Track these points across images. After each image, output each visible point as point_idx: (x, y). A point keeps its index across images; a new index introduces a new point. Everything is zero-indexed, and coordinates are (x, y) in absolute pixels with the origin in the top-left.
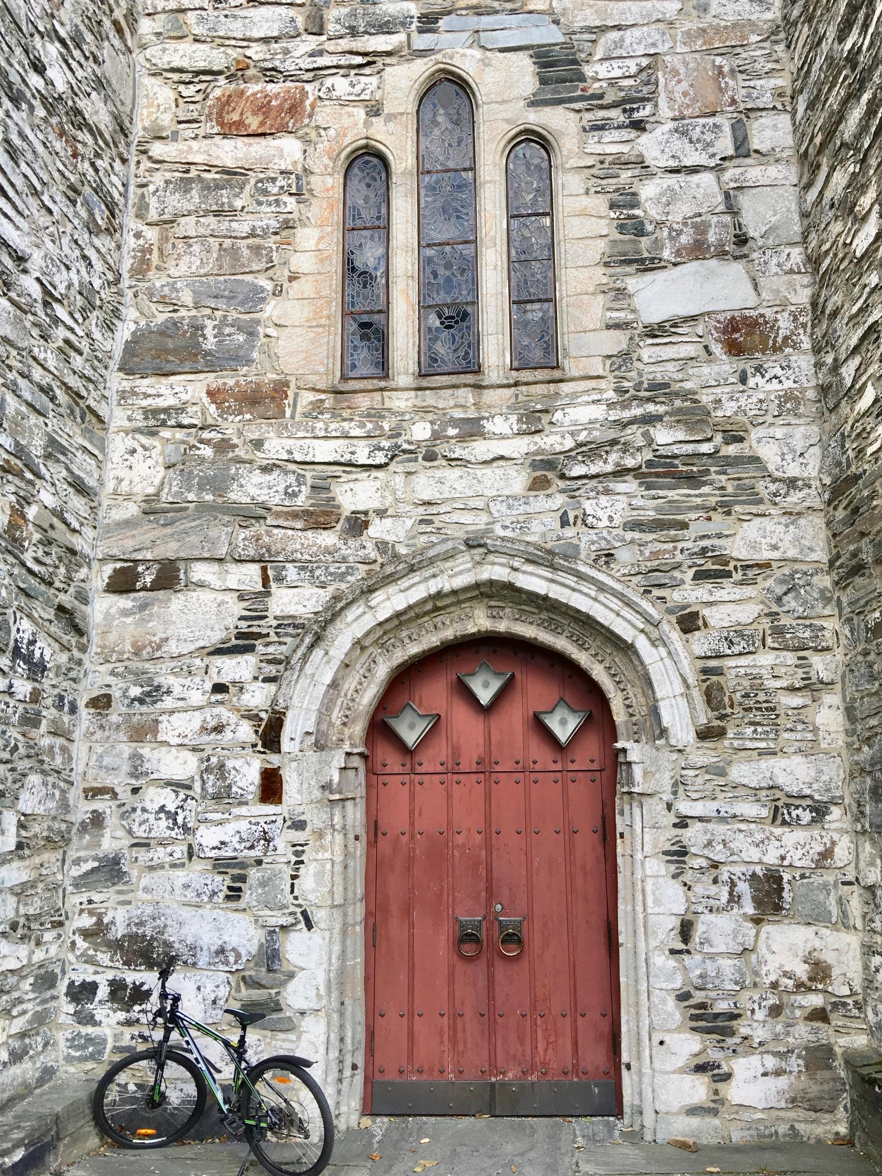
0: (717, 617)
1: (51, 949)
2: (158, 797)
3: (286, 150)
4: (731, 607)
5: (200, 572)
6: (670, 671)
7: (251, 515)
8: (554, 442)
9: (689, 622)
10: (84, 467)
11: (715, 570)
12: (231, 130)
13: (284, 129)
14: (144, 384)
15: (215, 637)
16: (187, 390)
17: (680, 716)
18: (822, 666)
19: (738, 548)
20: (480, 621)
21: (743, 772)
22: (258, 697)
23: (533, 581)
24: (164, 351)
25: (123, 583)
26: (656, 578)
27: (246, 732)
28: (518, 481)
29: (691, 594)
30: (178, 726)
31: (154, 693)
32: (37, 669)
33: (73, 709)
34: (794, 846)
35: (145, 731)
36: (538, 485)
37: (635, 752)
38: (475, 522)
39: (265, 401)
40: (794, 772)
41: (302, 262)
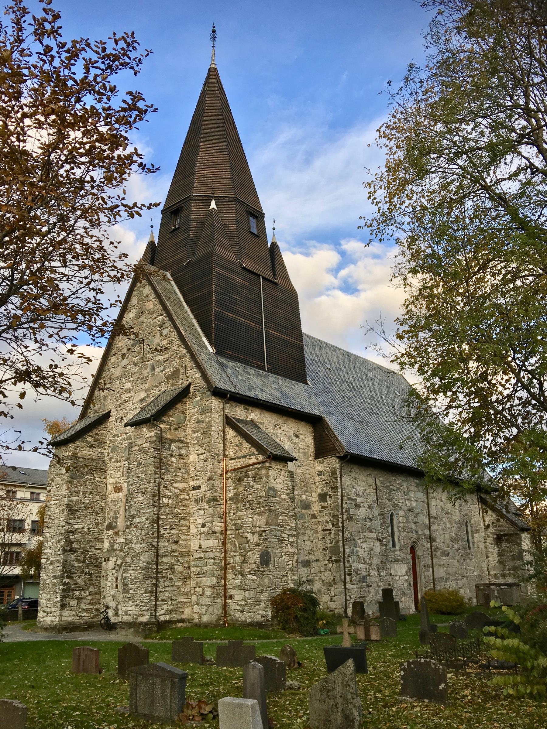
1: (98, 606)
2: (108, 588)
3: (120, 494)
5: (111, 559)
7: (115, 550)
10: (100, 546)
12: (116, 492)
13: (119, 492)
14: (108, 532)
15: (112, 567)
16: (110, 532)
22: (115, 575)
24: (110, 527)
25: (105, 561)
27: (114, 580)
30: (109, 579)
31: (107, 575)
32: (90, 574)
33: (100, 577)
35: (107, 580)
39: (117, 534)
41: (121, 513)
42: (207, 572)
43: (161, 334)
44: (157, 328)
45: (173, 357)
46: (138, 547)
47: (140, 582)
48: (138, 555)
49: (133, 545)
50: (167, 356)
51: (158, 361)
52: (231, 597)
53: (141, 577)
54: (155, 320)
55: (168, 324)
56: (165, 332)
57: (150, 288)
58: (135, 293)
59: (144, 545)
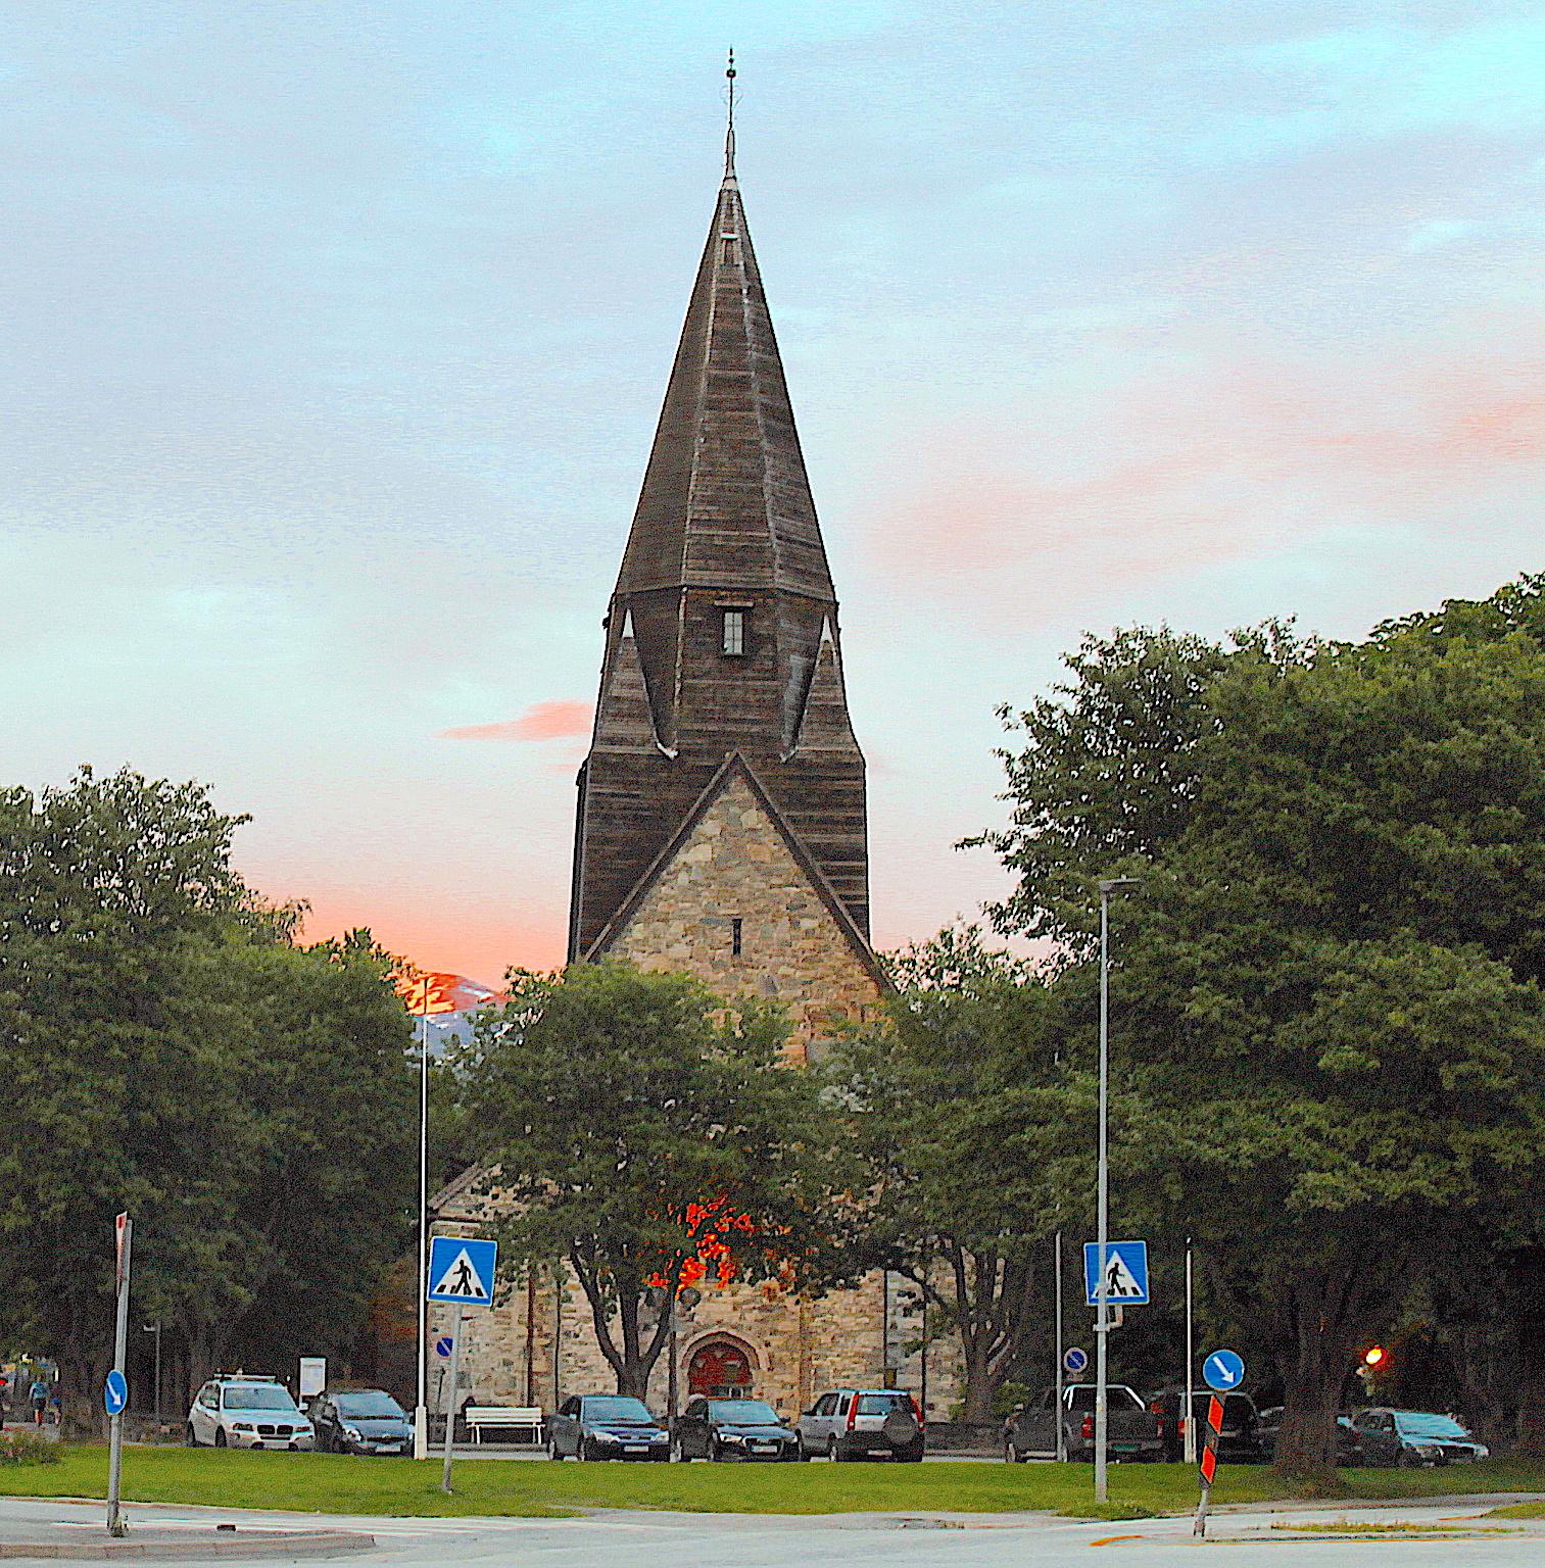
0: (773, 1344)
4: (776, 1341)
6: (763, 1354)
8: (737, 1298)
9: (767, 1345)
11: (774, 1332)
17: (764, 1366)
18: (795, 1356)
19: (780, 1328)
20: (719, 1339)
21: (776, 1377)
23: (732, 1332)
26: (760, 1334)
28: (730, 1308)
29: (768, 1338)
34: (785, 1393)
36: (735, 1309)
37: (753, 1372)
38: (719, 1318)
40: (787, 1378)
42: (907, 1365)
43: (794, 924)
44: (783, 908)
45: (827, 979)
46: (849, 1322)
47: (859, 1376)
48: (850, 1335)
49: (836, 1318)
50: (812, 973)
51: (785, 976)
52: (931, 1407)
53: (860, 1369)
54: (775, 891)
55: (814, 905)
56: (806, 924)
57: (763, 815)
58: (712, 811)
59: (867, 1320)
